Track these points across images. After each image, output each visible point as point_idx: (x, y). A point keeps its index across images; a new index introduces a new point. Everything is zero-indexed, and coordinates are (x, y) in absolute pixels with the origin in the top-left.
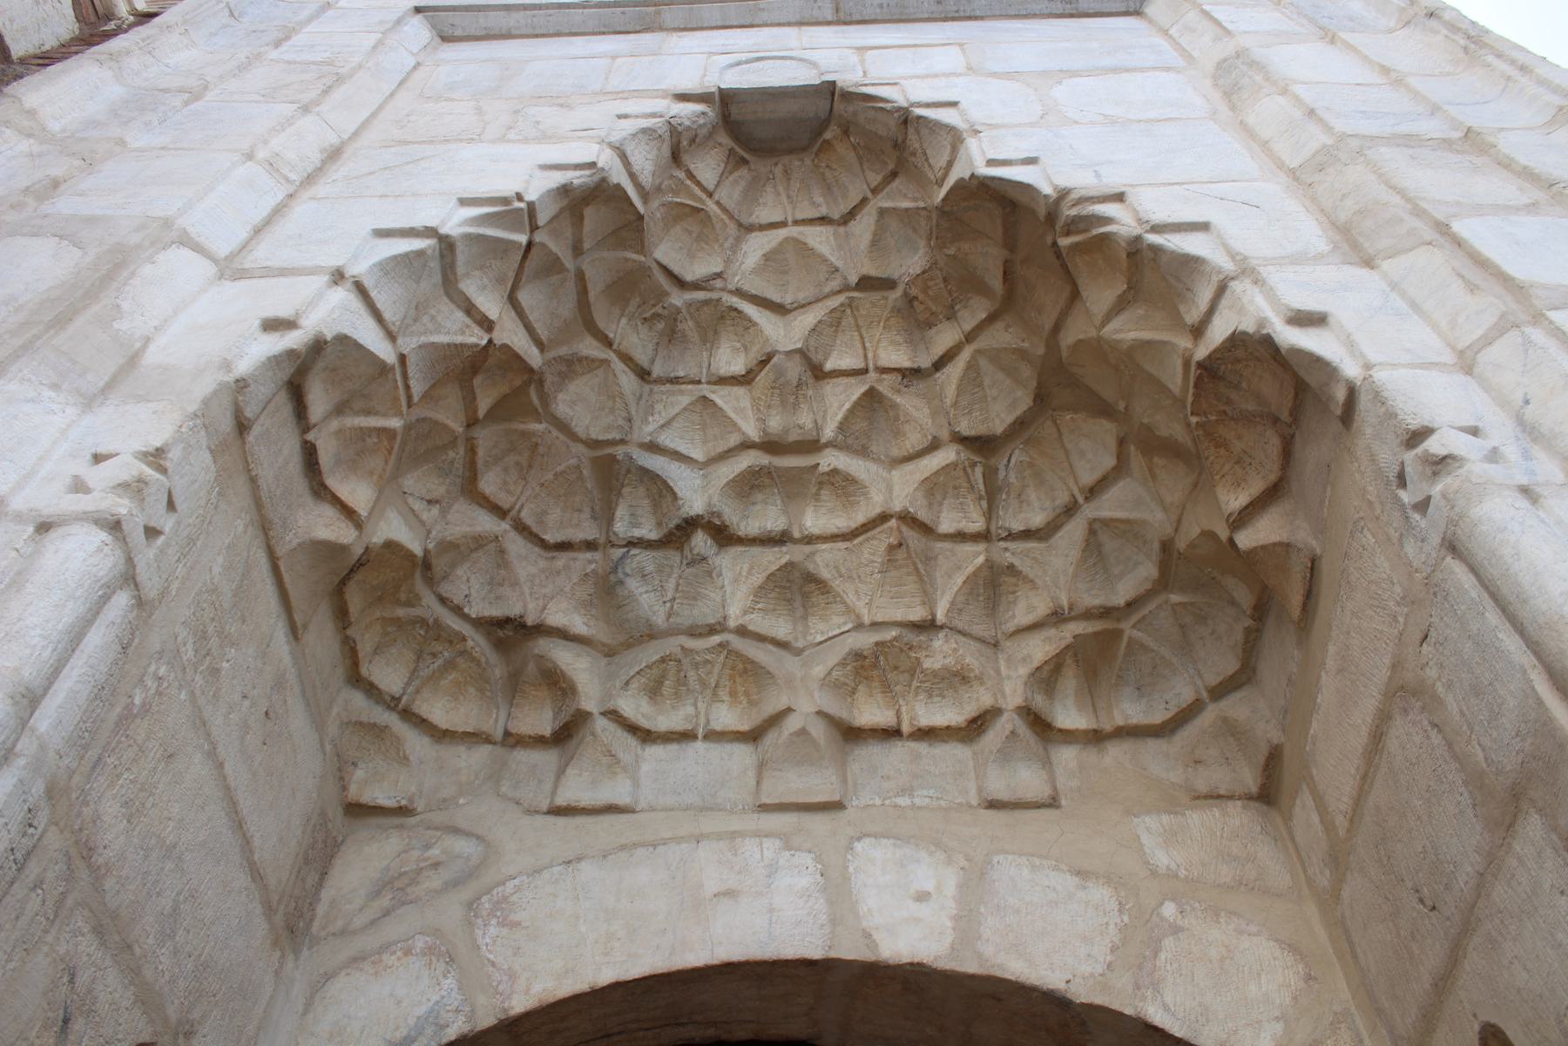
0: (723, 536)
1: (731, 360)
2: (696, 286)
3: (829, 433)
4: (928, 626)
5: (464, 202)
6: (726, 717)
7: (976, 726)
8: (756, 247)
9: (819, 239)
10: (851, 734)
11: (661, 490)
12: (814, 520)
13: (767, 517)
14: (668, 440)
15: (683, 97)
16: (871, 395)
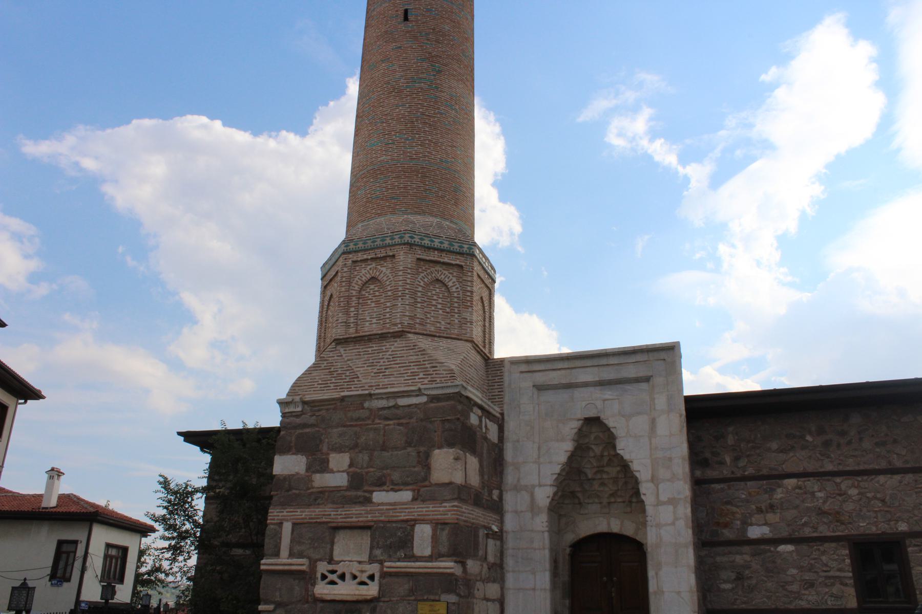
0: (594, 479)
1: (592, 454)
2: (586, 444)
3: (605, 464)
4: (618, 490)
5: (558, 464)
6: (596, 500)
7: (624, 502)
8: (592, 437)
9: (601, 435)
10: (609, 503)
11: (586, 475)
12: (605, 476)
13: (599, 476)
14: (586, 466)
15: (579, 420)
16: (610, 460)
